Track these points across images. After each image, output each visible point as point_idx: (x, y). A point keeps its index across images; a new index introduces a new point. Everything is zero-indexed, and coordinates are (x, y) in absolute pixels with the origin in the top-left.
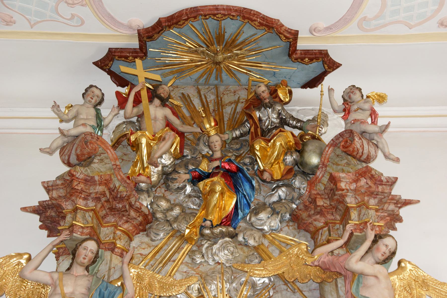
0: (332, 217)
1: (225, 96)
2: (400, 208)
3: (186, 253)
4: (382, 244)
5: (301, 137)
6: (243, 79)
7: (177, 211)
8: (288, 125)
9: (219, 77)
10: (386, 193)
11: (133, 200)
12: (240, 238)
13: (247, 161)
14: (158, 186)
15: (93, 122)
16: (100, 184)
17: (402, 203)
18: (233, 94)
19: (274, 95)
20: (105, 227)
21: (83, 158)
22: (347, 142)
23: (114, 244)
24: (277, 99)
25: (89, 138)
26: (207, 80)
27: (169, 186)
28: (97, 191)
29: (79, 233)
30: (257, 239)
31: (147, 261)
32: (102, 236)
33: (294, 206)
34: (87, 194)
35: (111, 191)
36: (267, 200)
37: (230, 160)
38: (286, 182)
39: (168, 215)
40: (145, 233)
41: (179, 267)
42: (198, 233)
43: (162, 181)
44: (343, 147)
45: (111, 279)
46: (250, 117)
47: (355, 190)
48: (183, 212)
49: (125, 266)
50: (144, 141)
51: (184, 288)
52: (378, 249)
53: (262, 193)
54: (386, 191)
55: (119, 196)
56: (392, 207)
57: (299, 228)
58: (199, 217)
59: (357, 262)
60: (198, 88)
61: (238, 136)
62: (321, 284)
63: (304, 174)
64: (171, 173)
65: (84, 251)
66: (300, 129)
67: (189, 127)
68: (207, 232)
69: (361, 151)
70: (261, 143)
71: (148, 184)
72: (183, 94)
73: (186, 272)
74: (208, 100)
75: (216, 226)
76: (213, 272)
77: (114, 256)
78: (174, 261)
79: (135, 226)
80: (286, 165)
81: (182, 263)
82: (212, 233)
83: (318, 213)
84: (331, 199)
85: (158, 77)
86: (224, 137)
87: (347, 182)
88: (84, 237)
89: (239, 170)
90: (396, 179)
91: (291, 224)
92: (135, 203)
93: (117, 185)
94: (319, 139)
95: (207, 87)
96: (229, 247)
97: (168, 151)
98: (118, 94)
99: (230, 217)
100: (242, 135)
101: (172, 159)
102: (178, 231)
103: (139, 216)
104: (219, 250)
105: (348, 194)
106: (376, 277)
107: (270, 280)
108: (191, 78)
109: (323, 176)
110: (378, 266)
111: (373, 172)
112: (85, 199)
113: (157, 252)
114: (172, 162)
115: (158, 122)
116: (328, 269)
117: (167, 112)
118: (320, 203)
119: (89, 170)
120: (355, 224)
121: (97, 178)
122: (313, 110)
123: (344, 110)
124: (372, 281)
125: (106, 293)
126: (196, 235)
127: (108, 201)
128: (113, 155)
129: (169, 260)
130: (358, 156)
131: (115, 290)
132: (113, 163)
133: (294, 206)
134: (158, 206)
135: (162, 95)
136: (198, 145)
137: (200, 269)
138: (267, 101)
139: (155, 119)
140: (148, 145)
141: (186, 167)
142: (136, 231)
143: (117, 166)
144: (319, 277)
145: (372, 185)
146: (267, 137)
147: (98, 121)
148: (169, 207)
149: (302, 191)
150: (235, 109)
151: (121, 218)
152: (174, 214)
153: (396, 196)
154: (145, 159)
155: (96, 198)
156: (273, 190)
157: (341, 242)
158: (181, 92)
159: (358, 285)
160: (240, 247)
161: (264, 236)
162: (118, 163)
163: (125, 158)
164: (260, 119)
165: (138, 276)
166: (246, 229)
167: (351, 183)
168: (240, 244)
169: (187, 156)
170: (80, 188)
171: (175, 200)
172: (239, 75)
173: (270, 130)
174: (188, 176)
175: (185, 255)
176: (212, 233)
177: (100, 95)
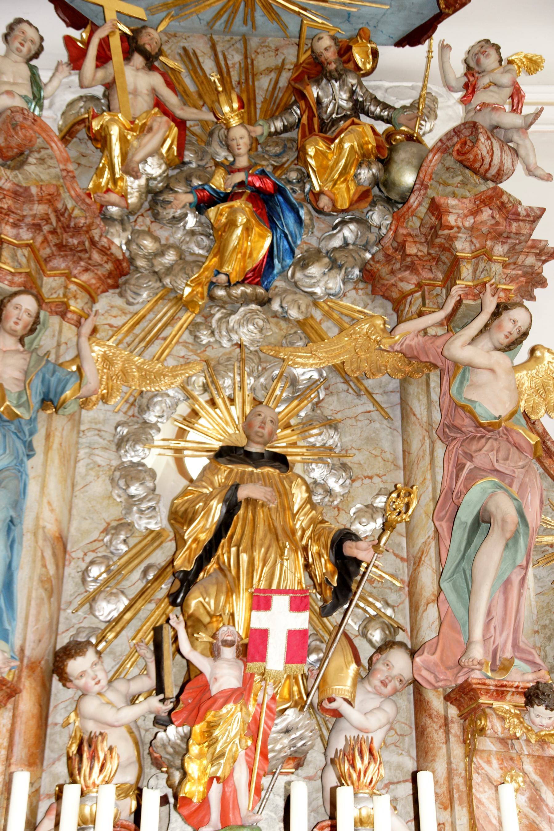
0: (431, 276)
1: (260, 57)
2: (544, 262)
3: (185, 326)
4: (507, 318)
5: (389, 136)
6: (293, 27)
7: (170, 257)
8: (367, 114)
9: (249, 19)
10: (523, 235)
11: (96, 233)
12: (276, 306)
13: (293, 176)
14: (139, 214)
15: (27, 91)
16: (40, 201)
18: (272, 54)
19: (345, 57)
20: (49, 276)
21: (10, 154)
22: (465, 143)
23: (66, 305)
24: (351, 65)
25: (19, 118)
26: (229, 22)
27: (158, 213)
28: (35, 212)
29: (6, 282)
30: (303, 308)
31: (120, 336)
32: (45, 291)
33: (368, 256)
34: (18, 217)
35: (59, 214)
36: (323, 244)
37: (263, 172)
38: (358, 215)
39: (155, 262)
40: (117, 291)
41: (173, 348)
42: (206, 294)
43: (146, 205)
44: (459, 153)
45: (61, 361)
46: (302, 96)
47: (472, 229)
48: (181, 259)
49: (84, 340)
50: (115, 131)
51: (179, 380)
52: (500, 327)
53: (317, 233)
54: (524, 232)
55: (72, 224)
56: (531, 260)
57: (374, 292)
58: (207, 269)
59: (463, 346)
60: (211, 39)
61: (279, 130)
62: (404, 382)
63: (389, 201)
64: (161, 192)
65: (16, 312)
66: (388, 121)
67: (195, 111)
68: (221, 293)
69: (487, 160)
70: (317, 144)
71: (122, 208)
72: (184, 49)
73: (183, 357)
74: (229, 63)
75: (235, 285)
76: (229, 359)
77: (66, 325)
78: (165, 339)
79: (100, 278)
80: (358, 184)
81: (178, 342)
82: (229, 295)
83: (407, 268)
84: (430, 244)
85: (139, 12)
86: (255, 132)
87: (459, 216)
88: (15, 289)
89: (280, 190)
90: (543, 210)
91: (361, 285)
92: (100, 239)
93: (70, 206)
94: (419, 141)
95: (228, 38)
96: (256, 320)
97: (156, 152)
98: (69, 41)
99: (260, 270)
100: (286, 129)
101: (164, 167)
102: (173, 290)
103: (106, 262)
104: (240, 324)
105: (460, 235)
106: (492, 370)
107: (321, 375)
108: (200, 19)
109: (420, 204)
110: (498, 355)
111: (505, 198)
112: (15, 225)
113: (137, 323)
114: (164, 172)
115: (140, 99)
116: (416, 358)
117: (157, 80)
118: (411, 249)
119: (20, 176)
120: (467, 286)
121: (34, 190)
122: (412, 88)
123: (466, 86)
124: (483, 377)
125: (53, 381)
126: (203, 298)
127: (53, 232)
128: (61, 152)
129: (156, 336)
130: (482, 171)
131: (68, 377)
132: (62, 167)
133: (368, 256)
134: (139, 247)
135: (148, 47)
136: (209, 144)
137: (207, 353)
138: (333, 66)
139: (135, 93)
140: (123, 139)
141: (188, 180)
142: (102, 287)
143: (68, 172)
144: (400, 371)
145: (501, 221)
146: (329, 135)
147: (35, 89)
148: (157, 249)
149: (384, 231)
150: (277, 82)
151: (76, 263)
152: (167, 261)
153: (540, 241)
154: (117, 161)
155: (34, 225)
156: (334, 228)
157: (441, 315)
158: (182, 45)
159: (461, 383)
160: (275, 320)
161: (316, 304)
162: (71, 167)
163: (83, 161)
164: (319, 101)
165: (106, 358)
166: (285, 291)
167: (466, 216)
168: (275, 315)
169: (190, 162)
170: (6, 206)
171: (167, 239)
172: (285, 17)
173: (335, 122)
174: (190, 198)
175: (183, 329)
176: (229, 295)
177: (37, 40)
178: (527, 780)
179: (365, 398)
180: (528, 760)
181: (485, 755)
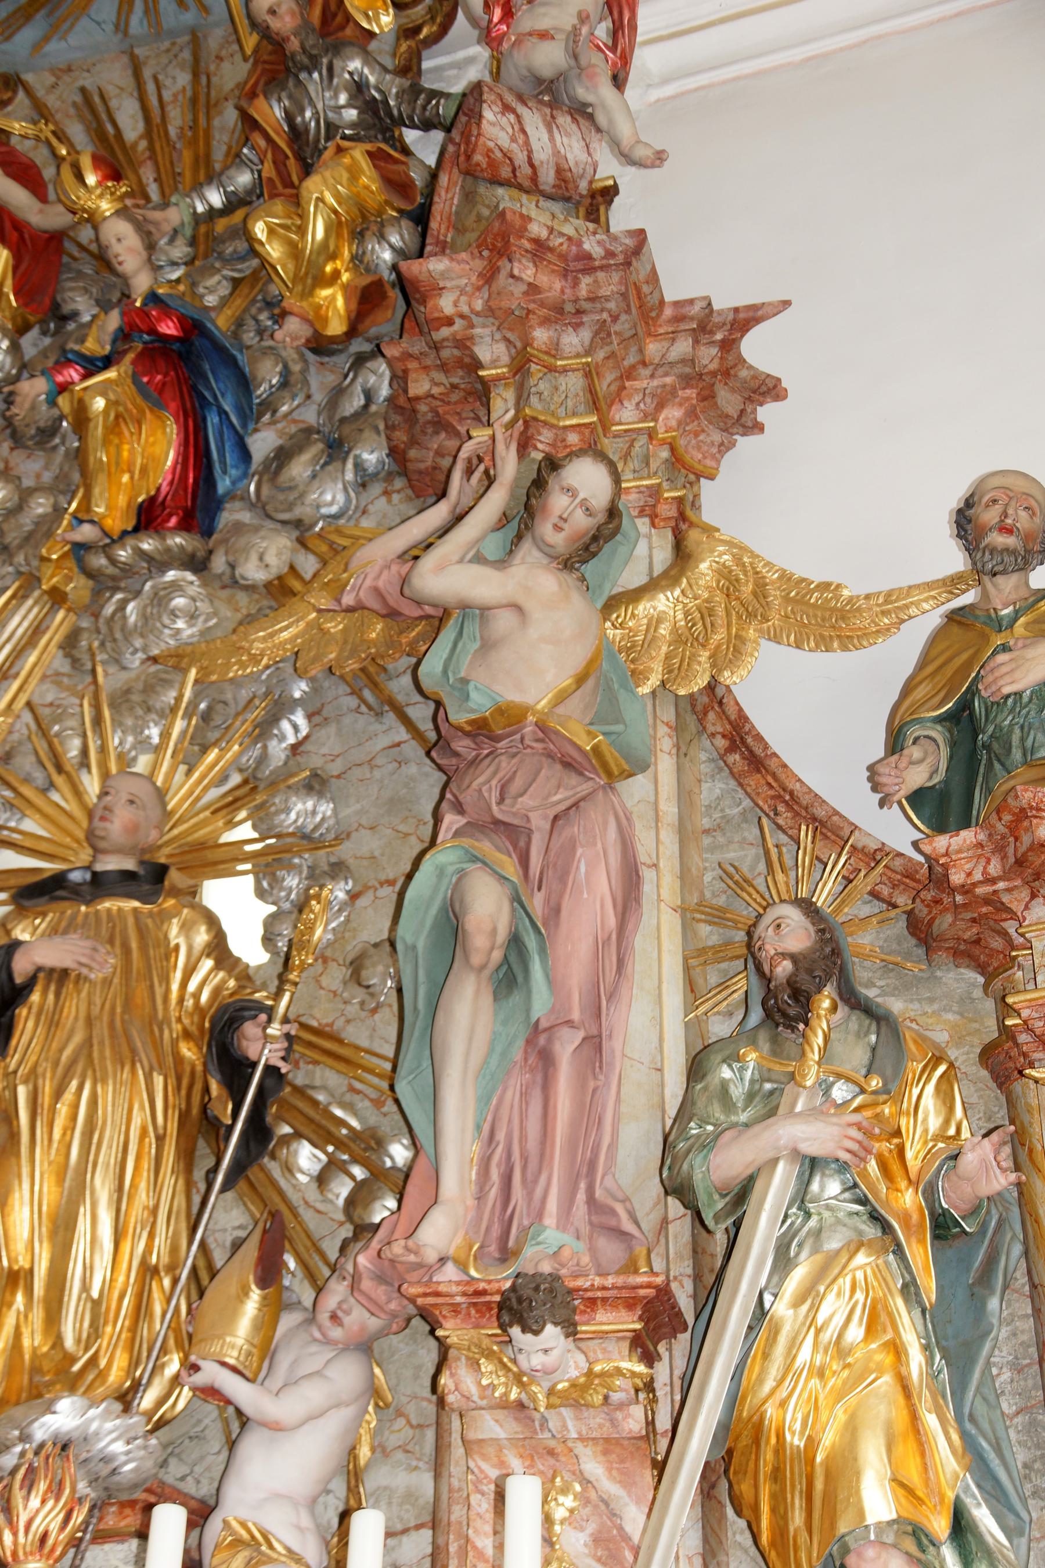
4: (557, 487)
10: (607, 299)
17: (724, 324)
69: (520, 158)
72: (83, 90)
73: (51, 704)
74: (167, 96)
86: (166, 220)
87: (463, 292)
95: (166, 44)
105: (477, 331)
108: (98, 23)
153: (691, 302)
158: (80, 83)
178: (593, 1495)
179: (391, 718)
180: (588, 1451)
181: (490, 1451)
